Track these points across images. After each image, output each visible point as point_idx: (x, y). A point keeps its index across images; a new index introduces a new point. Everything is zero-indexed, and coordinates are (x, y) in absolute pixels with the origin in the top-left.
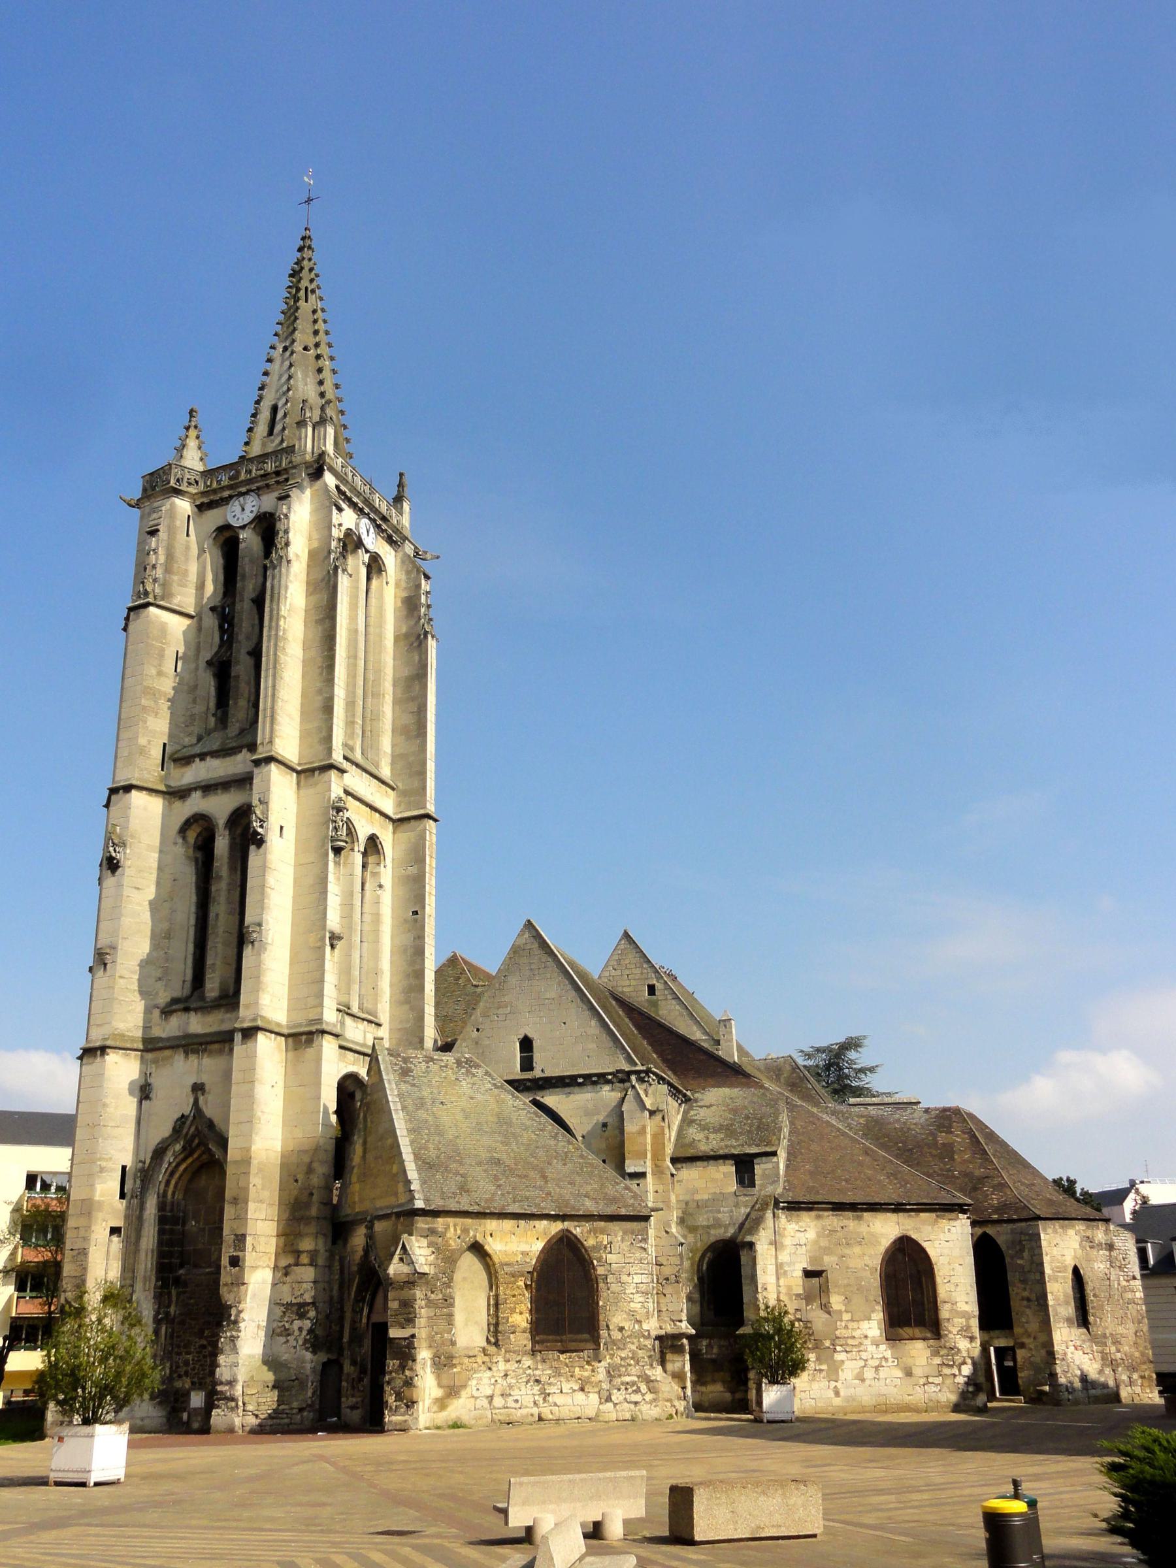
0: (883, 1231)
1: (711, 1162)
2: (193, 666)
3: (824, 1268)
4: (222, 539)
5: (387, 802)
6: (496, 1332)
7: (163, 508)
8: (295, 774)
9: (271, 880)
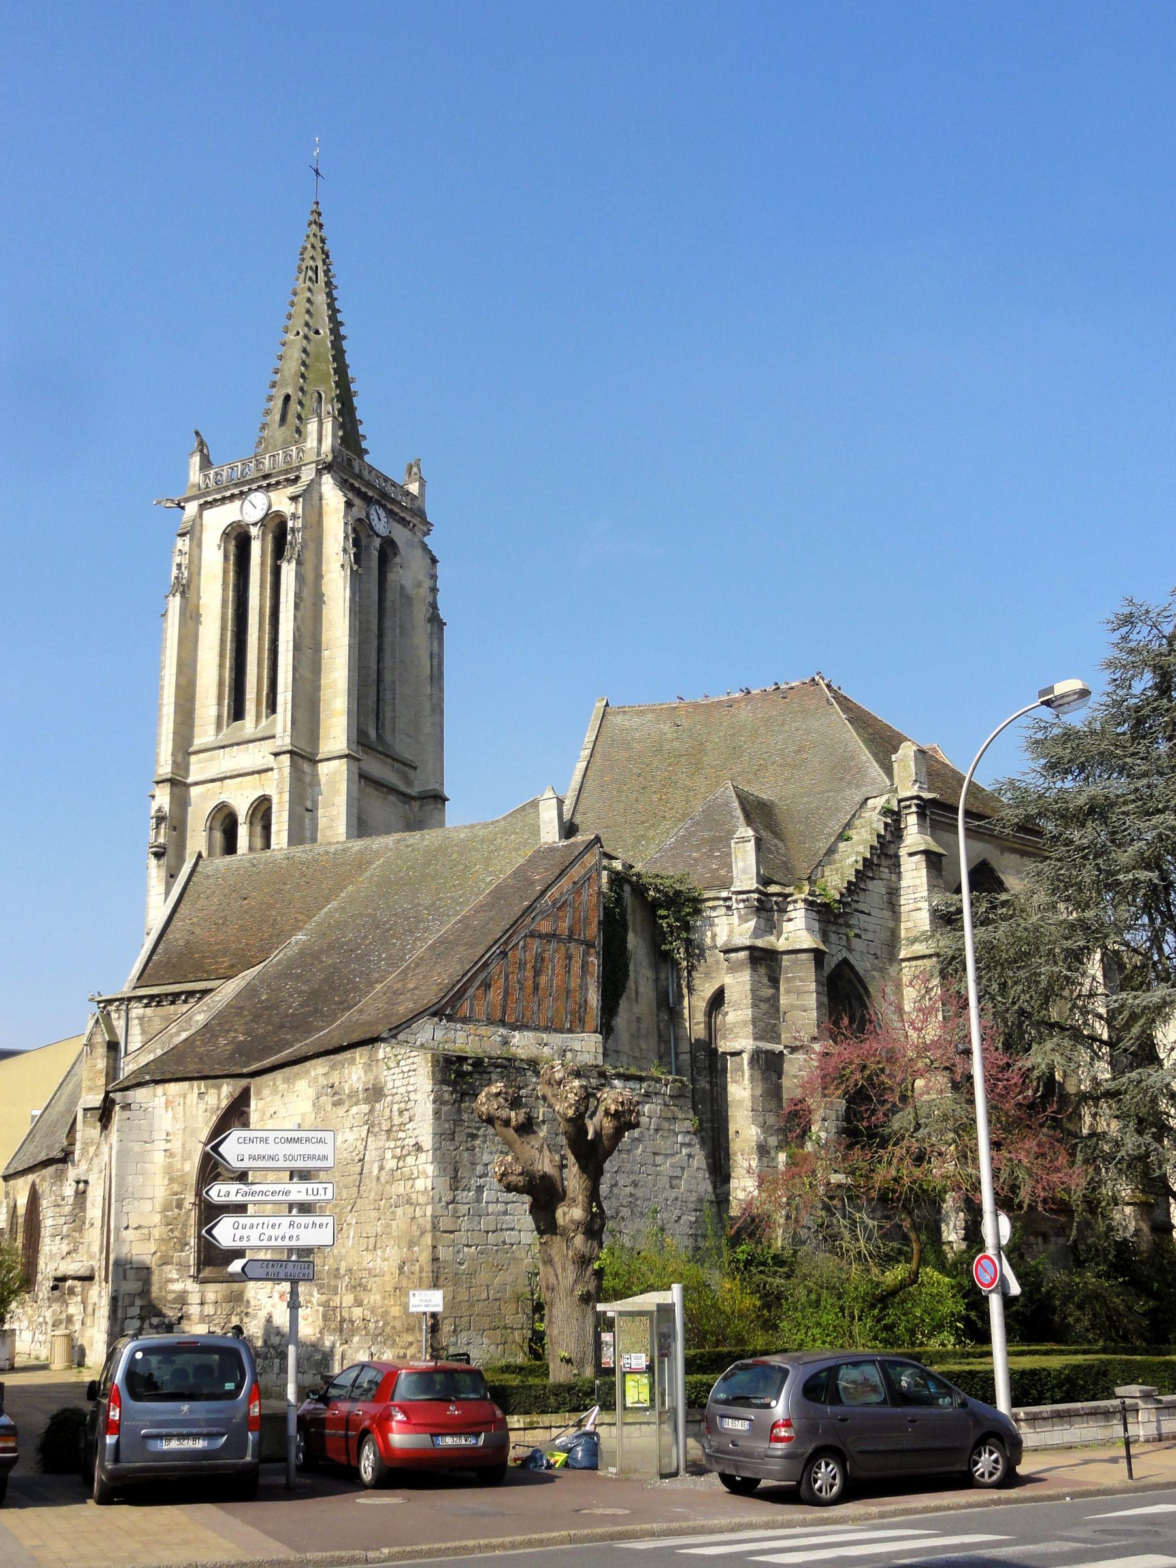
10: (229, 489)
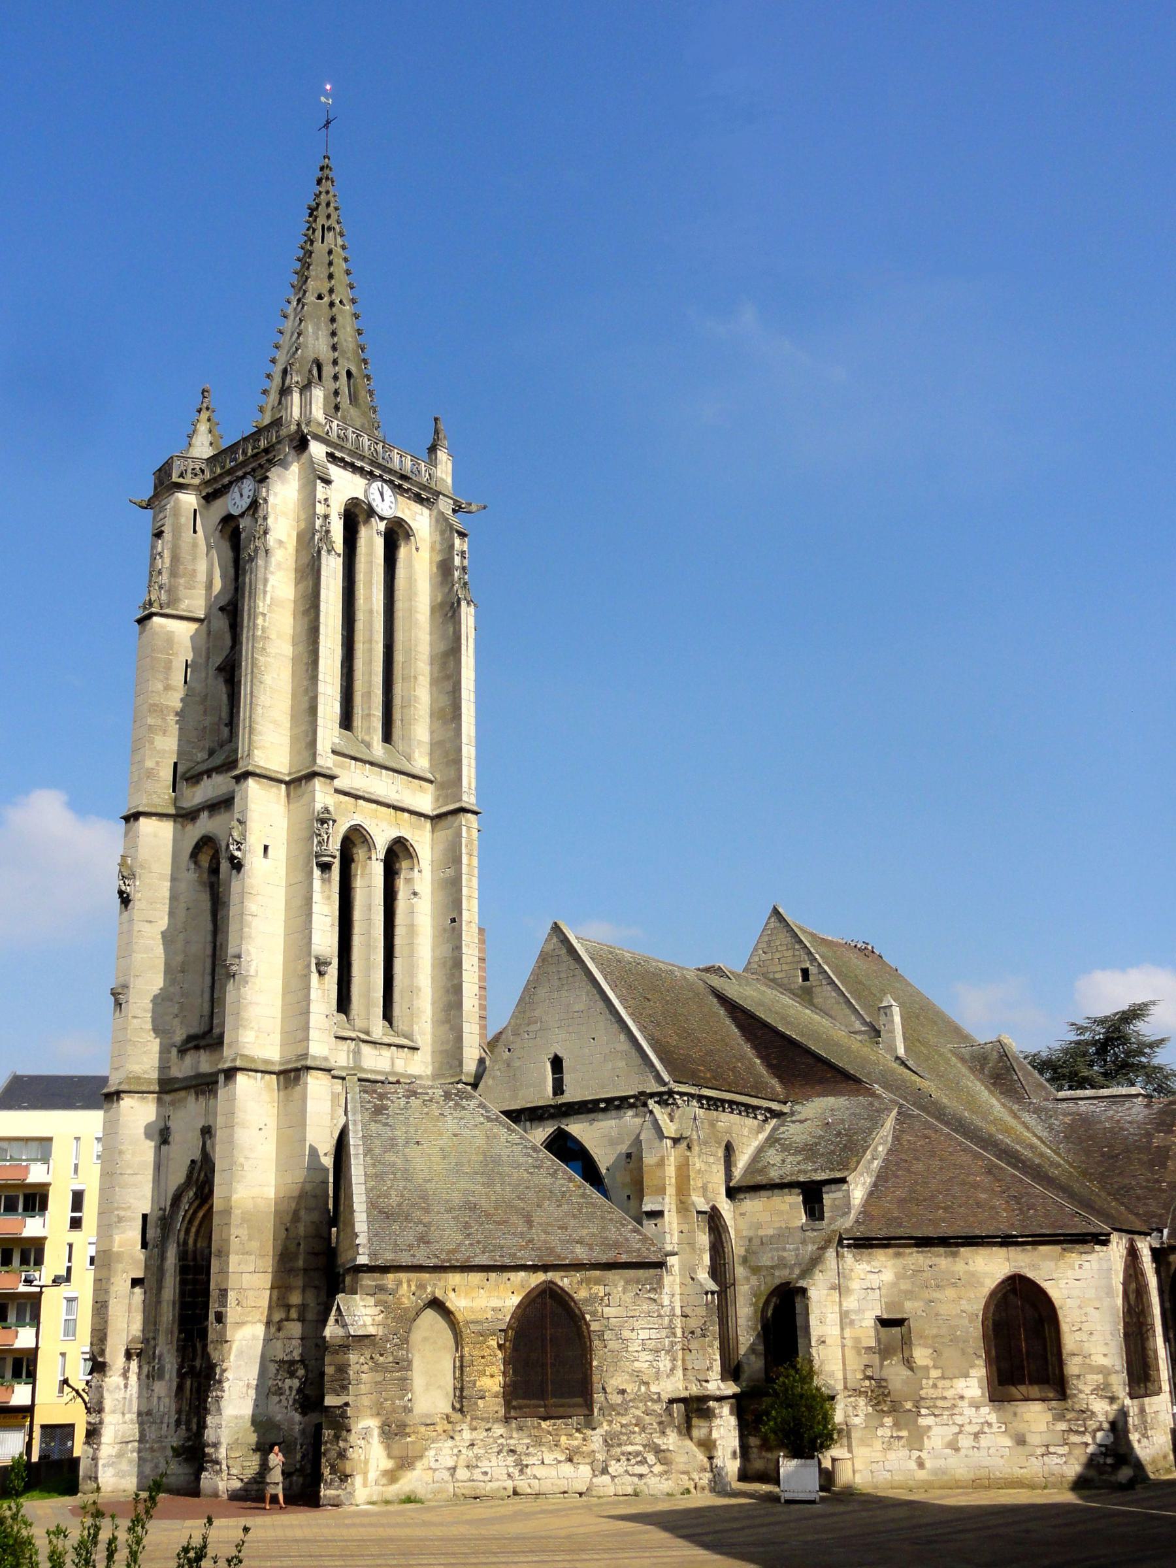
0: (987, 1269)
1: (776, 1191)
2: (203, 675)
3: (905, 1316)
5: (425, 800)
6: (461, 1397)
7: (168, 507)
8: (283, 786)
9: (252, 906)
10: (362, 460)
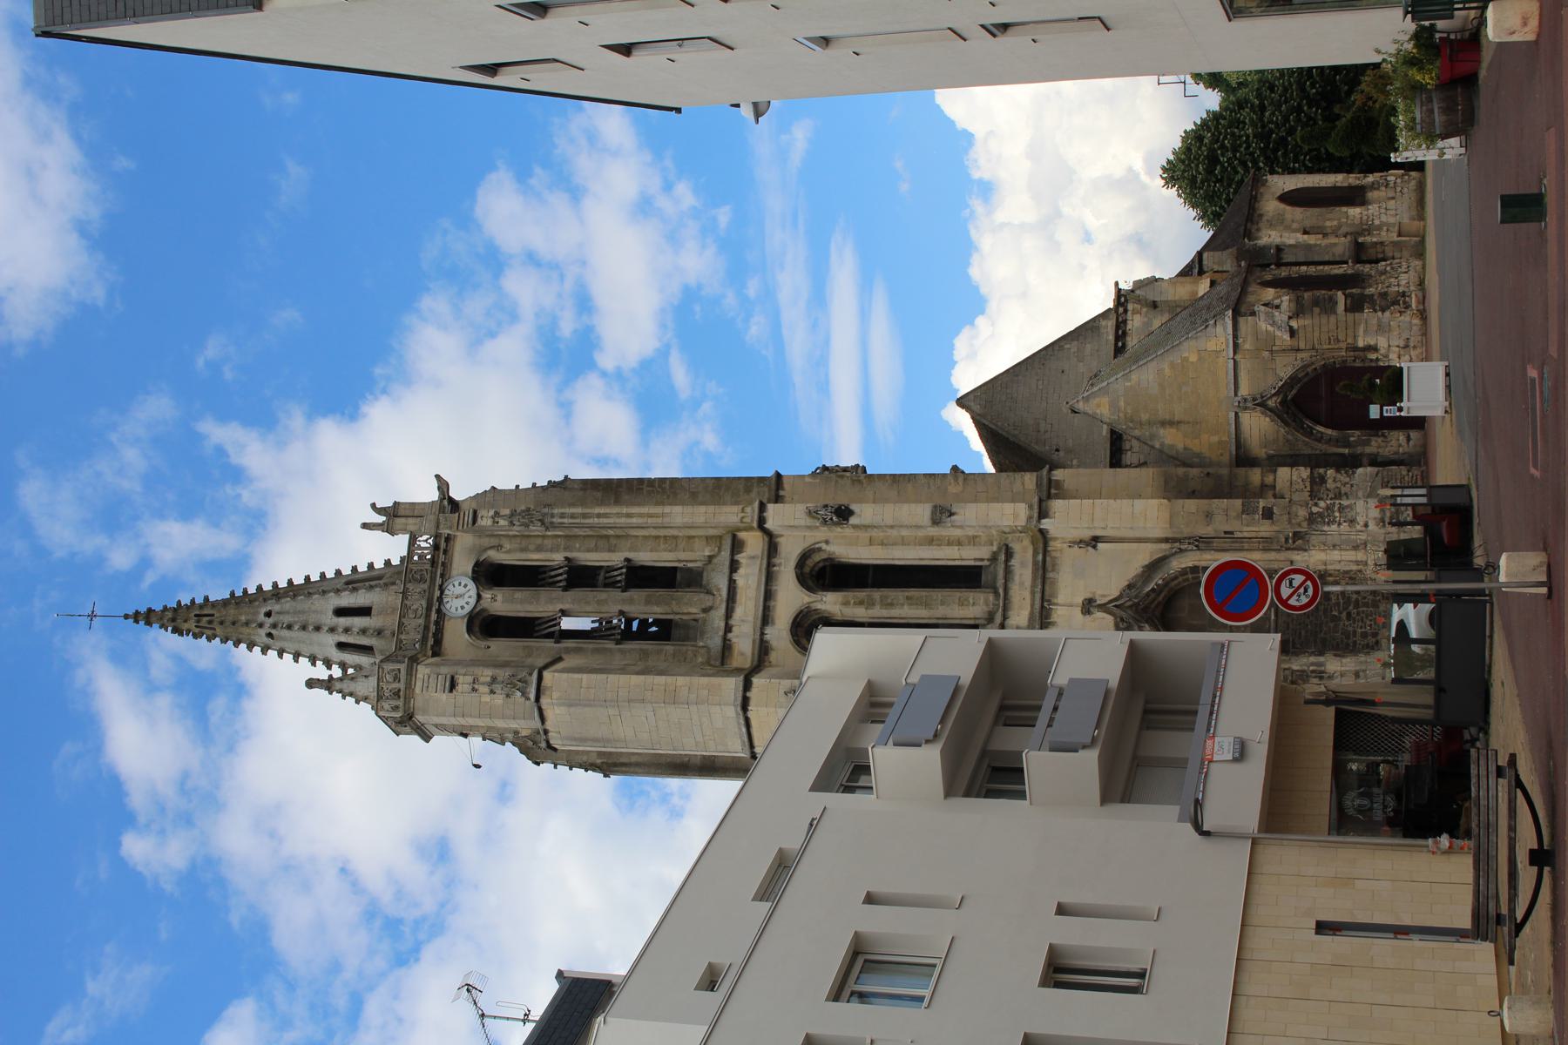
4: (479, 634)
